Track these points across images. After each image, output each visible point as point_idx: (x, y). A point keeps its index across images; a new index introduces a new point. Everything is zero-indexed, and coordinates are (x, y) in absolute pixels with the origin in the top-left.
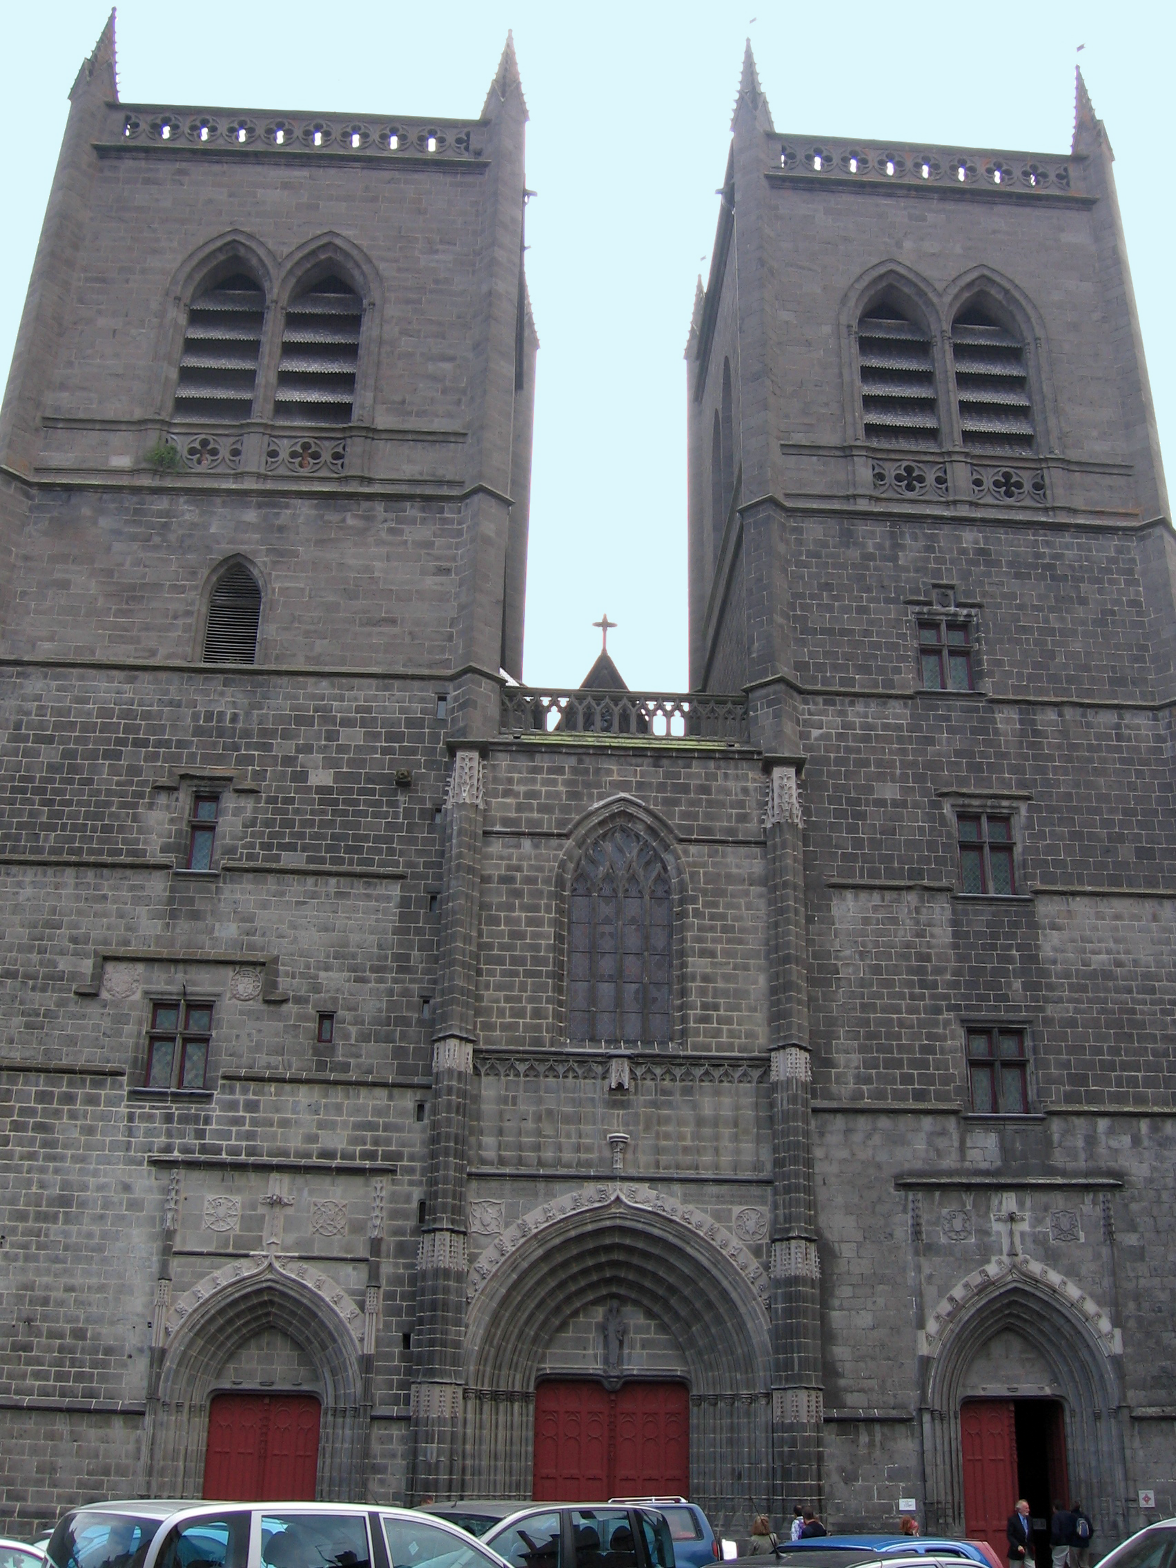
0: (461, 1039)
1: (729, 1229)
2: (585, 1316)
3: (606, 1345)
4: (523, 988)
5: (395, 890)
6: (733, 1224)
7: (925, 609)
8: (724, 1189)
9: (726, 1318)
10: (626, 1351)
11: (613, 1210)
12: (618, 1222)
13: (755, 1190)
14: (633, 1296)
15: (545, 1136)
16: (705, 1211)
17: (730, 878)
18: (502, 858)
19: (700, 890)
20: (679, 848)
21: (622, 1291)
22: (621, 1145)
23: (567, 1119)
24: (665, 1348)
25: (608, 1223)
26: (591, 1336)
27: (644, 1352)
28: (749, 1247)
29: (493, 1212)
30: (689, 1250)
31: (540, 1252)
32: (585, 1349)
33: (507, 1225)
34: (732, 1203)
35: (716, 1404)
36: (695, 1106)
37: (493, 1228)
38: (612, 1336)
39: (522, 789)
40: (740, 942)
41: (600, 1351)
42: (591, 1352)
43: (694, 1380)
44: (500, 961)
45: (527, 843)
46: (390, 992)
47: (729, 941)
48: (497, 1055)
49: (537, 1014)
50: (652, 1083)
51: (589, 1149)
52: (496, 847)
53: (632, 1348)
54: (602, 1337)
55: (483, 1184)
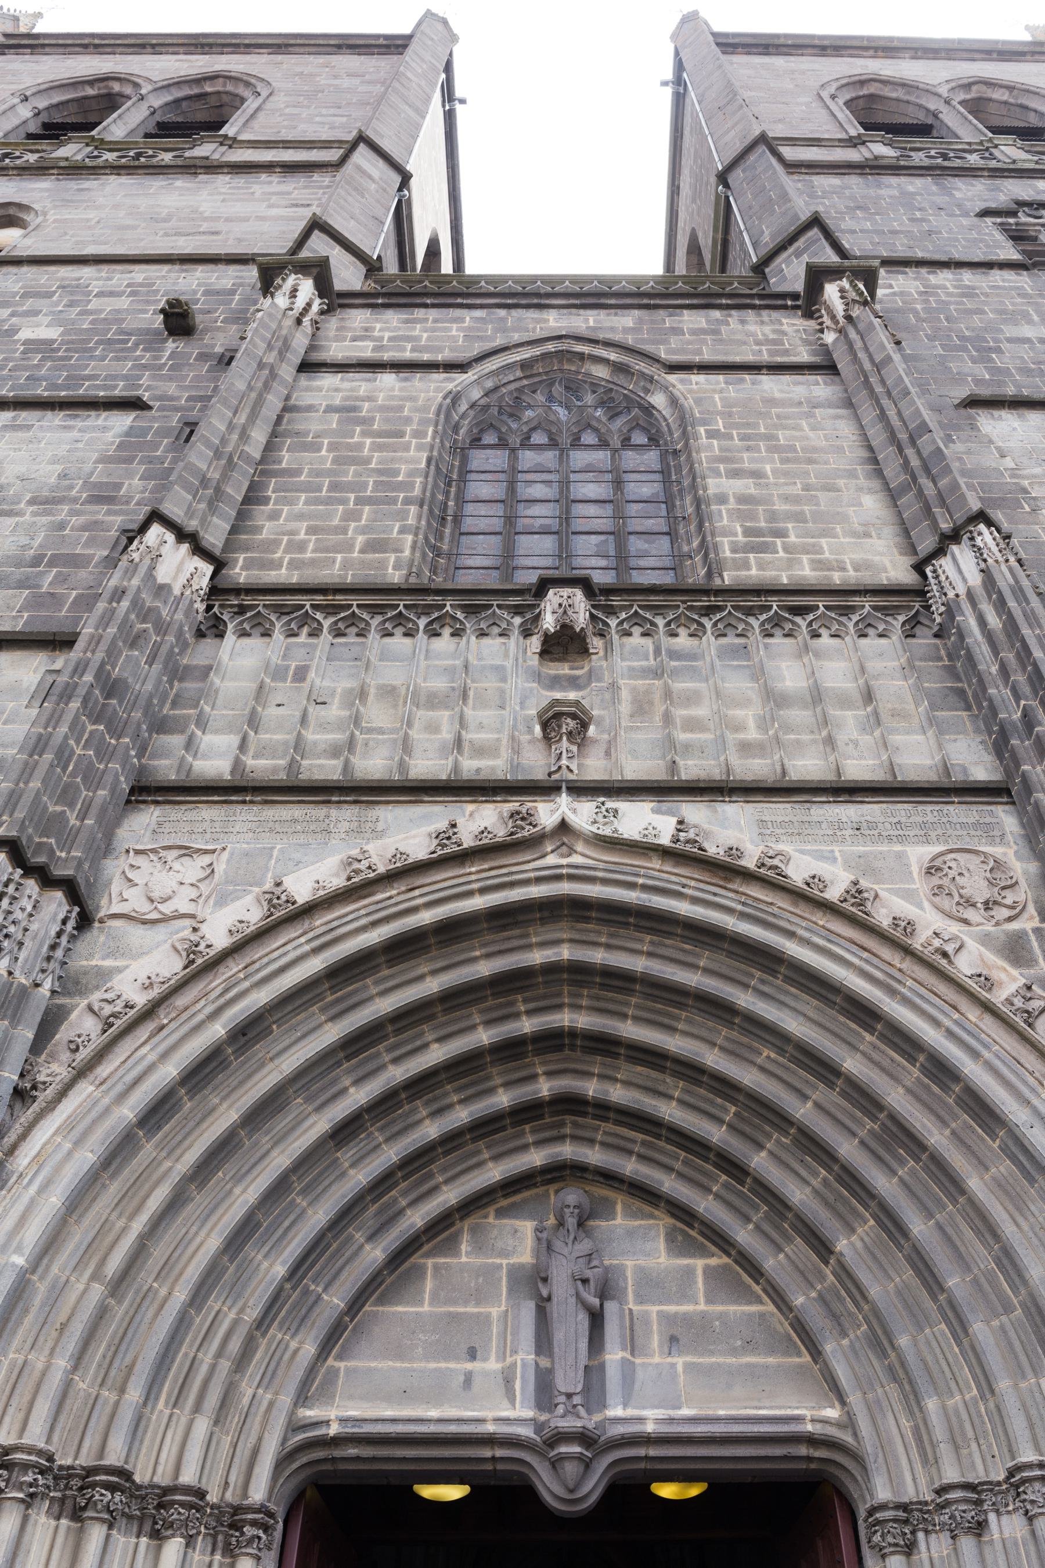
0: (182, 535)
1: (908, 895)
2: (479, 1248)
3: (543, 1342)
4: (351, 516)
5: (122, 421)
6: (920, 885)
7: (1011, 220)
8: (871, 811)
9: (957, 1160)
10: (614, 1356)
11: (551, 860)
12: (566, 888)
13: (958, 812)
14: (630, 1167)
15: (370, 731)
16: (820, 856)
17: (771, 402)
18: (337, 390)
19: (719, 413)
20: (673, 378)
21: (594, 1156)
22: (571, 724)
23: (433, 701)
24: (749, 1345)
25: (536, 891)
26: (495, 1312)
27: (680, 1361)
28: (985, 940)
29: (192, 869)
30: (792, 949)
31: (316, 965)
32: (472, 1354)
33: (222, 901)
34: (901, 839)
35: (979, 1528)
36: (758, 674)
37: (183, 906)
38: (561, 1287)
39: (387, 335)
40: (810, 461)
41: (525, 1356)
42: (493, 1365)
43: (869, 1446)
44: (308, 488)
45: (388, 379)
46: (62, 526)
47: (783, 461)
48: (270, 599)
49: (374, 546)
50: (648, 642)
51: (480, 751)
52: (328, 381)
53: (632, 1345)
54: (528, 1311)
55: (174, 813)
